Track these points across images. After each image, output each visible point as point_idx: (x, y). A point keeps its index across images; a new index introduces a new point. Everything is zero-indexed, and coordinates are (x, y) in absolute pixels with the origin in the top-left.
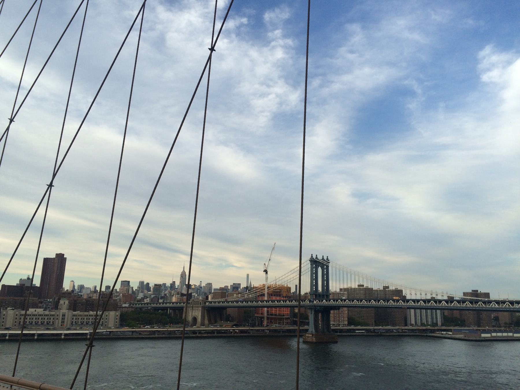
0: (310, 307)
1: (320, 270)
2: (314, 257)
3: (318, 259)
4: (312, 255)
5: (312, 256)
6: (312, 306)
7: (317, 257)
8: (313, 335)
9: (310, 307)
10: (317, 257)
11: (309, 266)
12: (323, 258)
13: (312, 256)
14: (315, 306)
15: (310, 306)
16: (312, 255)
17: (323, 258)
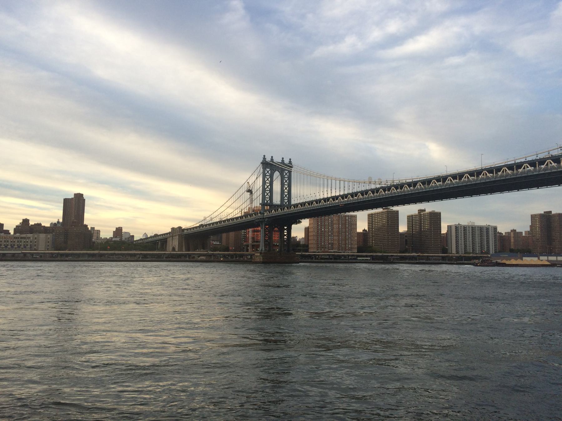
0: (259, 220)
1: (277, 174)
2: (268, 159)
3: (273, 162)
4: (264, 156)
5: (264, 158)
6: (261, 219)
7: (272, 159)
8: (261, 253)
9: (259, 220)
10: (272, 159)
12: (283, 161)
13: (264, 158)
14: (263, 218)
16: (264, 156)
17: (283, 161)
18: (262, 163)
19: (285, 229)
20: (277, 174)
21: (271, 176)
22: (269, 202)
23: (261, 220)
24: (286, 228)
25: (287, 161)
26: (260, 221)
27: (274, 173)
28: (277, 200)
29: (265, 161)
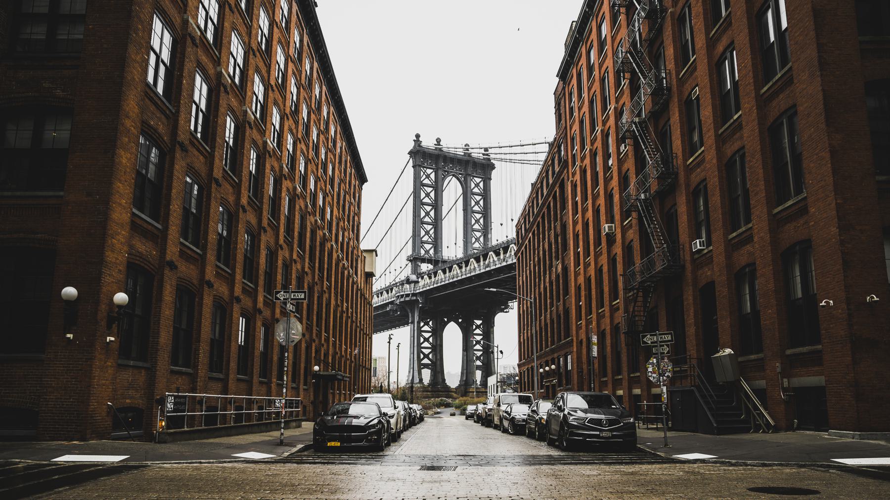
2: (428, 142)
4: (418, 136)
9: (402, 300)
11: (410, 171)
15: (402, 296)
16: (418, 136)
18: (411, 153)
19: (478, 327)
20: (452, 189)
21: (438, 188)
22: (432, 252)
23: (407, 299)
24: (479, 322)
25: (477, 154)
26: (405, 301)
27: (443, 179)
28: (453, 248)
29: (420, 146)
